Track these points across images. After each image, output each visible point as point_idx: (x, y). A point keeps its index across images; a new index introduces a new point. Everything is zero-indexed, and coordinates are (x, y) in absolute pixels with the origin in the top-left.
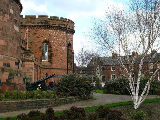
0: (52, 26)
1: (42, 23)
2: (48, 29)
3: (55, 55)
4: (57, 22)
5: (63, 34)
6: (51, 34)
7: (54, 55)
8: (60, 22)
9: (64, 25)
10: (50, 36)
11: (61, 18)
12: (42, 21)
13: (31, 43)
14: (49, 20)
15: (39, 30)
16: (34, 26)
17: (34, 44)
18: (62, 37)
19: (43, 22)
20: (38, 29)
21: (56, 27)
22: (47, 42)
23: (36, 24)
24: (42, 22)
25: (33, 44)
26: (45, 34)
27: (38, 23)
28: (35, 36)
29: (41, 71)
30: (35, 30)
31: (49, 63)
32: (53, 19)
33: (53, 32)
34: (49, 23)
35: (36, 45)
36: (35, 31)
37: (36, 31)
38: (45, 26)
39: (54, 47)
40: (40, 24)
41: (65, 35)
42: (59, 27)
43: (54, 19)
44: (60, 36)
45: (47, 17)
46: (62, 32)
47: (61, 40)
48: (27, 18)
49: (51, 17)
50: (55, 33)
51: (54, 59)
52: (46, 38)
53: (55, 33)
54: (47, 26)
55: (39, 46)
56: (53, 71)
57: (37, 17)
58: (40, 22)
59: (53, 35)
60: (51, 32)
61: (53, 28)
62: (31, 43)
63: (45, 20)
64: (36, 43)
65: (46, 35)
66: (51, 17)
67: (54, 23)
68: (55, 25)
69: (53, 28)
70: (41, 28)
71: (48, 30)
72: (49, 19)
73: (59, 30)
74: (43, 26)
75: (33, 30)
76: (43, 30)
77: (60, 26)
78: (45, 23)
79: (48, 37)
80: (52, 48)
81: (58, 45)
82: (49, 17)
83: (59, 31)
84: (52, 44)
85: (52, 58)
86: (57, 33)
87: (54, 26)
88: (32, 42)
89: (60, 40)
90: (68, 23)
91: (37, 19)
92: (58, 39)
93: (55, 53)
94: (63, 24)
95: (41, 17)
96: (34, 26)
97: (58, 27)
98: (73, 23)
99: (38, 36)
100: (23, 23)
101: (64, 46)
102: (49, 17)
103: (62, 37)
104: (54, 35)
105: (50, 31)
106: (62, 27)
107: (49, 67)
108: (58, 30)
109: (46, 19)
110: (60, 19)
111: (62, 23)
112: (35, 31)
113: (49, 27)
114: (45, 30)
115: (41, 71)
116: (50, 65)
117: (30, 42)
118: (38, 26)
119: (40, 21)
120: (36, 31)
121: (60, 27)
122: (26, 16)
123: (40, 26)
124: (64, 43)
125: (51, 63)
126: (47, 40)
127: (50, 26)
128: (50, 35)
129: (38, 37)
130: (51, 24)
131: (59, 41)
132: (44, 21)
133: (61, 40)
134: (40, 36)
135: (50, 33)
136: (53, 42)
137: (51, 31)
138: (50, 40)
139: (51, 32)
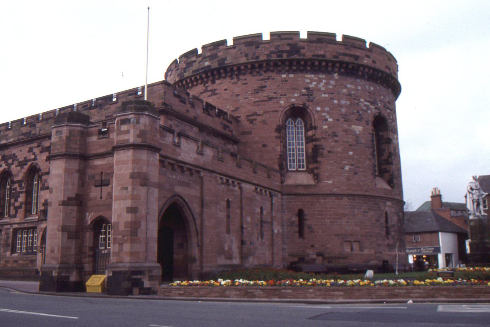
1: (280, 53)
2: (302, 71)
3: (329, 152)
5: (353, 87)
6: (310, 86)
7: (325, 152)
8: (342, 50)
9: (357, 57)
10: (310, 92)
12: (281, 49)
13: (252, 118)
14: (301, 44)
15: (273, 75)
16: (257, 65)
17: (259, 119)
18: (350, 95)
19: (283, 52)
20: (270, 74)
21: (327, 62)
22: (297, 112)
23: (263, 58)
24: (279, 51)
25: (255, 119)
27: (268, 55)
29: (272, 204)
30: (262, 77)
31: (310, 176)
32: (315, 38)
33: (320, 81)
34: (302, 51)
35: (264, 122)
36: (262, 80)
37: (264, 80)
38: (291, 62)
39: (325, 127)
40: (274, 57)
41: (359, 88)
42: (337, 62)
44: (345, 91)
47: (348, 103)
48: (239, 44)
49: (310, 34)
50: (327, 84)
51: (326, 166)
52: (295, 99)
53: (324, 81)
54: (298, 61)
56: (322, 201)
57: (266, 37)
58: (272, 52)
59: (319, 90)
60: (310, 79)
61: (319, 66)
62: (252, 118)
63: (288, 45)
65: (295, 89)
66: (310, 34)
67: (322, 52)
68: (324, 56)
69: (316, 68)
70: (279, 68)
71: (300, 74)
72: (303, 41)
74: (283, 62)
75: (256, 78)
76: (284, 76)
77: (341, 58)
78: (290, 53)
79: (303, 95)
80: (315, 128)
81: (338, 120)
82: (304, 36)
83: (339, 74)
84: (316, 116)
85: (319, 159)
86: (333, 82)
88: (252, 115)
89: (343, 102)
90: (368, 53)
91: (267, 42)
92: (336, 102)
93: (327, 145)
94: (351, 56)
96: (257, 65)
97: (334, 63)
98: (390, 59)
99: (272, 95)
100: (226, 62)
101: (358, 122)
102: (304, 36)
103: (350, 95)
104: (323, 89)
105: (307, 78)
106: (347, 64)
107: (311, 191)
108: (335, 72)
111: (347, 52)
112: (262, 80)
113: (302, 63)
114: (292, 76)
115: (272, 204)
116: (312, 182)
117: (247, 116)
119: (273, 49)
120: (264, 80)
121: (341, 63)
122: (236, 40)
124: (358, 112)
125: (317, 177)
127: (306, 61)
128: (307, 89)
129: (270, 99)
131: (340, 106)
132: (288, 48)
133: (348, 103)
134: (275, 95)
135: (308, 83)
136: (318, 109)
137: (313, 76)
138: (307, 104)
139: (312, 80)
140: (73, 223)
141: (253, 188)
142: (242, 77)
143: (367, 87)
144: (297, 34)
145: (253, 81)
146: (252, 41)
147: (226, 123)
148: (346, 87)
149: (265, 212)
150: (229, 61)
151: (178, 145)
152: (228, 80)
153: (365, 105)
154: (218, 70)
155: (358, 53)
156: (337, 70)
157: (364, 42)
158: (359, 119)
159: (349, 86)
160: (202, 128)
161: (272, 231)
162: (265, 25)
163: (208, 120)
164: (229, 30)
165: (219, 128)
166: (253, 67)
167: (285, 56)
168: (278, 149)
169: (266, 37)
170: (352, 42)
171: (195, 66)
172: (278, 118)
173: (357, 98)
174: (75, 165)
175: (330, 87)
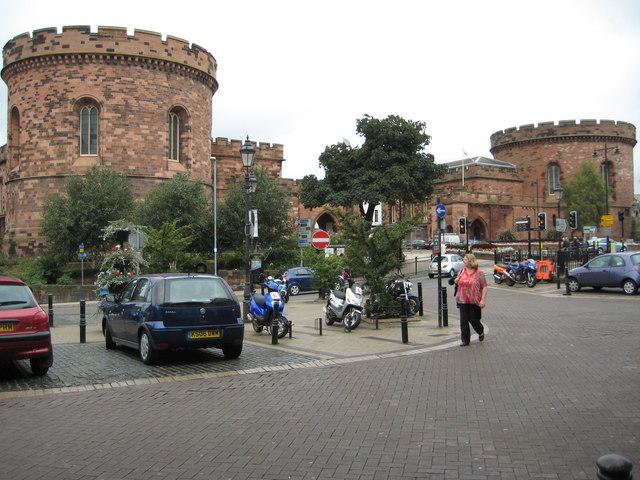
1: (543, 135)
9: (588, 132)
46: (586, 144)
52: (552, 158)
55: (540, 173)
57: (536, 126)
60: (564, 148)
82: (556, 124)
102: (556, 124)
123: (540, 140)
126: (554, 160)
145: (530, 149)
146: (528, 129)
150: (518, 139)
155: (588, 128)
157: (595, 121)
160: (498, 180)
162: (535, 120)
163: (501, 176)
164: (518, 123)
165: (510, 178)
167: (546, 137)
169: (536, 126)
170: (586, 124)
172: (544, 169)
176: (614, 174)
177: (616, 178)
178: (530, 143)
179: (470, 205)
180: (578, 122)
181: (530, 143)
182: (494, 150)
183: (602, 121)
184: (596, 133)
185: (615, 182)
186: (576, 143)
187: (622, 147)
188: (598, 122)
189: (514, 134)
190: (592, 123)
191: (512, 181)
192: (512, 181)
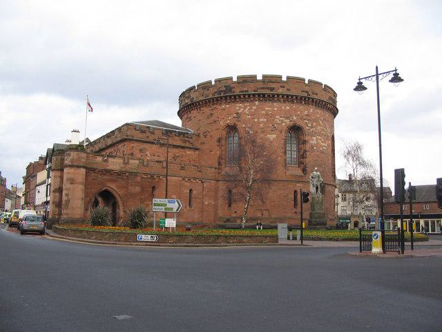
0: (239, 96)
4: (252, 85)
5: (270, 109)
9: (272, 89)
11: (264, 77)
14: (233, 85)
19: (222, 91)
20: (215, 106)
21: (249, 95)
23: (211, 96)
26: (227, 113)
27: (213, 95)
28: (211, 120)
29: (203, 187)
33: (245, 108)
34: (233, 90)
38: (226, 97)
40: (217, 96)
43: (246, 80)
45: (231, 78)
47: (265, 120)
50: (251, 109)
54: (230, 97)
55: (216, 138)
60: (239, 107)
64: (212, 133)
72: (235, 83)
73: (259, 100)
74: (221, 98)
77: (259, 92)
78: (225, 92)
82: (235, 79)
87: (244, 96)
92: (256, 120)
94: (268, 88)
95: (218, 81)
97: (254, 95)
102: (235, 79)
106: (264, 95)
109: (229, 82)
110: (306, 82)
111: (265, 86)
118: (213, 99)
119: (216, 90)
121: (259, 95)
127: (235, 96)
130: (237, 91)
131: (259, 123)
133: (265, 120)
135: (238, 110)
136: (244, 126)
139: (240, 108)
140: (57, 200)
141: (181, 179)
142: (202, 109)
143: (283, 107)
144: (231, 78)
145: (206, 110)
146: (205, 86)
147: (186, 139)
148: (264, 110)
149: (194, 192)
151: (106, 161)
152: (196, 111)
153: (280, 120)
154: (190, 105)
155: (273, 85)
156: (257, 99)
158: (274, 129)
159: (266, 109)
161: (203, 203)
162: (212, 76)
165: (179, 143)
166: (206, 103)
168: (218, 153)
170: (269, 79)
171: (183, 103)
173: (273, 116)
174: (58, 173)
175: (252, 110)
176: (305, 142)
177: (307, 147)
178: (207, 102)
179: (90, 170)
180: (259, 78)
181: (207, 102)
182: (180, 114)
183: (288, 78)
184: (280, 91)
185: (305, 151)
186: (257, 103)
187: (319, 113)
188: (284, 79)
189: (193, 95)
190: (276, 79)
191: (183, 147)
192: (183, 147)
